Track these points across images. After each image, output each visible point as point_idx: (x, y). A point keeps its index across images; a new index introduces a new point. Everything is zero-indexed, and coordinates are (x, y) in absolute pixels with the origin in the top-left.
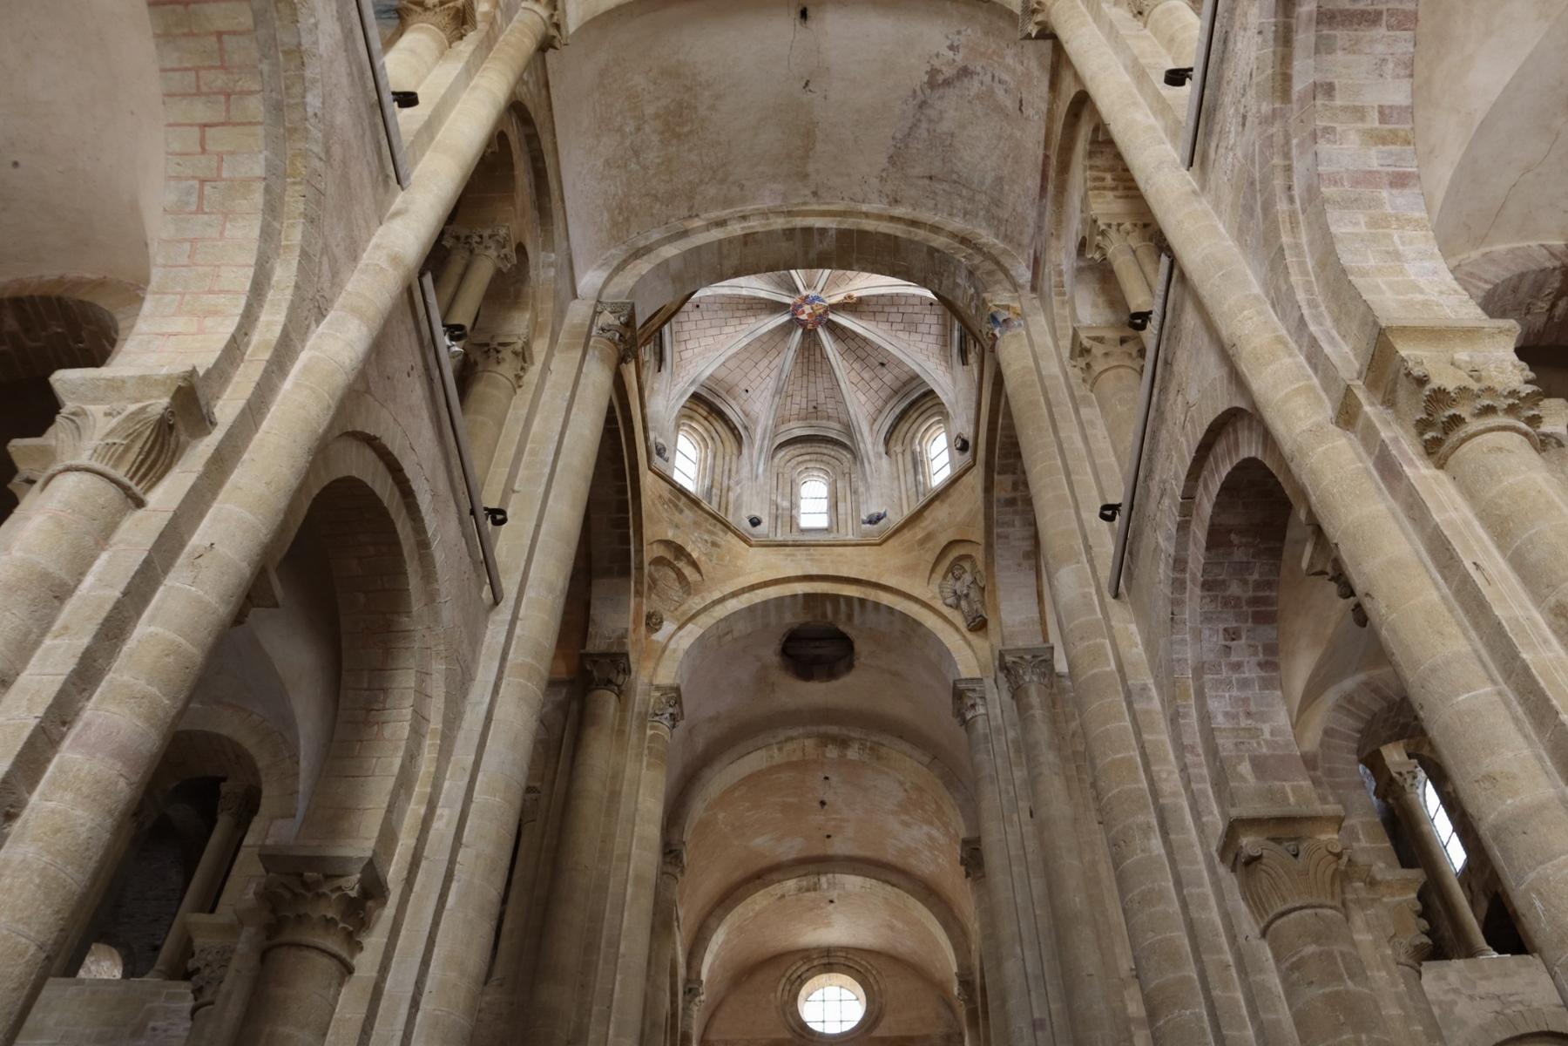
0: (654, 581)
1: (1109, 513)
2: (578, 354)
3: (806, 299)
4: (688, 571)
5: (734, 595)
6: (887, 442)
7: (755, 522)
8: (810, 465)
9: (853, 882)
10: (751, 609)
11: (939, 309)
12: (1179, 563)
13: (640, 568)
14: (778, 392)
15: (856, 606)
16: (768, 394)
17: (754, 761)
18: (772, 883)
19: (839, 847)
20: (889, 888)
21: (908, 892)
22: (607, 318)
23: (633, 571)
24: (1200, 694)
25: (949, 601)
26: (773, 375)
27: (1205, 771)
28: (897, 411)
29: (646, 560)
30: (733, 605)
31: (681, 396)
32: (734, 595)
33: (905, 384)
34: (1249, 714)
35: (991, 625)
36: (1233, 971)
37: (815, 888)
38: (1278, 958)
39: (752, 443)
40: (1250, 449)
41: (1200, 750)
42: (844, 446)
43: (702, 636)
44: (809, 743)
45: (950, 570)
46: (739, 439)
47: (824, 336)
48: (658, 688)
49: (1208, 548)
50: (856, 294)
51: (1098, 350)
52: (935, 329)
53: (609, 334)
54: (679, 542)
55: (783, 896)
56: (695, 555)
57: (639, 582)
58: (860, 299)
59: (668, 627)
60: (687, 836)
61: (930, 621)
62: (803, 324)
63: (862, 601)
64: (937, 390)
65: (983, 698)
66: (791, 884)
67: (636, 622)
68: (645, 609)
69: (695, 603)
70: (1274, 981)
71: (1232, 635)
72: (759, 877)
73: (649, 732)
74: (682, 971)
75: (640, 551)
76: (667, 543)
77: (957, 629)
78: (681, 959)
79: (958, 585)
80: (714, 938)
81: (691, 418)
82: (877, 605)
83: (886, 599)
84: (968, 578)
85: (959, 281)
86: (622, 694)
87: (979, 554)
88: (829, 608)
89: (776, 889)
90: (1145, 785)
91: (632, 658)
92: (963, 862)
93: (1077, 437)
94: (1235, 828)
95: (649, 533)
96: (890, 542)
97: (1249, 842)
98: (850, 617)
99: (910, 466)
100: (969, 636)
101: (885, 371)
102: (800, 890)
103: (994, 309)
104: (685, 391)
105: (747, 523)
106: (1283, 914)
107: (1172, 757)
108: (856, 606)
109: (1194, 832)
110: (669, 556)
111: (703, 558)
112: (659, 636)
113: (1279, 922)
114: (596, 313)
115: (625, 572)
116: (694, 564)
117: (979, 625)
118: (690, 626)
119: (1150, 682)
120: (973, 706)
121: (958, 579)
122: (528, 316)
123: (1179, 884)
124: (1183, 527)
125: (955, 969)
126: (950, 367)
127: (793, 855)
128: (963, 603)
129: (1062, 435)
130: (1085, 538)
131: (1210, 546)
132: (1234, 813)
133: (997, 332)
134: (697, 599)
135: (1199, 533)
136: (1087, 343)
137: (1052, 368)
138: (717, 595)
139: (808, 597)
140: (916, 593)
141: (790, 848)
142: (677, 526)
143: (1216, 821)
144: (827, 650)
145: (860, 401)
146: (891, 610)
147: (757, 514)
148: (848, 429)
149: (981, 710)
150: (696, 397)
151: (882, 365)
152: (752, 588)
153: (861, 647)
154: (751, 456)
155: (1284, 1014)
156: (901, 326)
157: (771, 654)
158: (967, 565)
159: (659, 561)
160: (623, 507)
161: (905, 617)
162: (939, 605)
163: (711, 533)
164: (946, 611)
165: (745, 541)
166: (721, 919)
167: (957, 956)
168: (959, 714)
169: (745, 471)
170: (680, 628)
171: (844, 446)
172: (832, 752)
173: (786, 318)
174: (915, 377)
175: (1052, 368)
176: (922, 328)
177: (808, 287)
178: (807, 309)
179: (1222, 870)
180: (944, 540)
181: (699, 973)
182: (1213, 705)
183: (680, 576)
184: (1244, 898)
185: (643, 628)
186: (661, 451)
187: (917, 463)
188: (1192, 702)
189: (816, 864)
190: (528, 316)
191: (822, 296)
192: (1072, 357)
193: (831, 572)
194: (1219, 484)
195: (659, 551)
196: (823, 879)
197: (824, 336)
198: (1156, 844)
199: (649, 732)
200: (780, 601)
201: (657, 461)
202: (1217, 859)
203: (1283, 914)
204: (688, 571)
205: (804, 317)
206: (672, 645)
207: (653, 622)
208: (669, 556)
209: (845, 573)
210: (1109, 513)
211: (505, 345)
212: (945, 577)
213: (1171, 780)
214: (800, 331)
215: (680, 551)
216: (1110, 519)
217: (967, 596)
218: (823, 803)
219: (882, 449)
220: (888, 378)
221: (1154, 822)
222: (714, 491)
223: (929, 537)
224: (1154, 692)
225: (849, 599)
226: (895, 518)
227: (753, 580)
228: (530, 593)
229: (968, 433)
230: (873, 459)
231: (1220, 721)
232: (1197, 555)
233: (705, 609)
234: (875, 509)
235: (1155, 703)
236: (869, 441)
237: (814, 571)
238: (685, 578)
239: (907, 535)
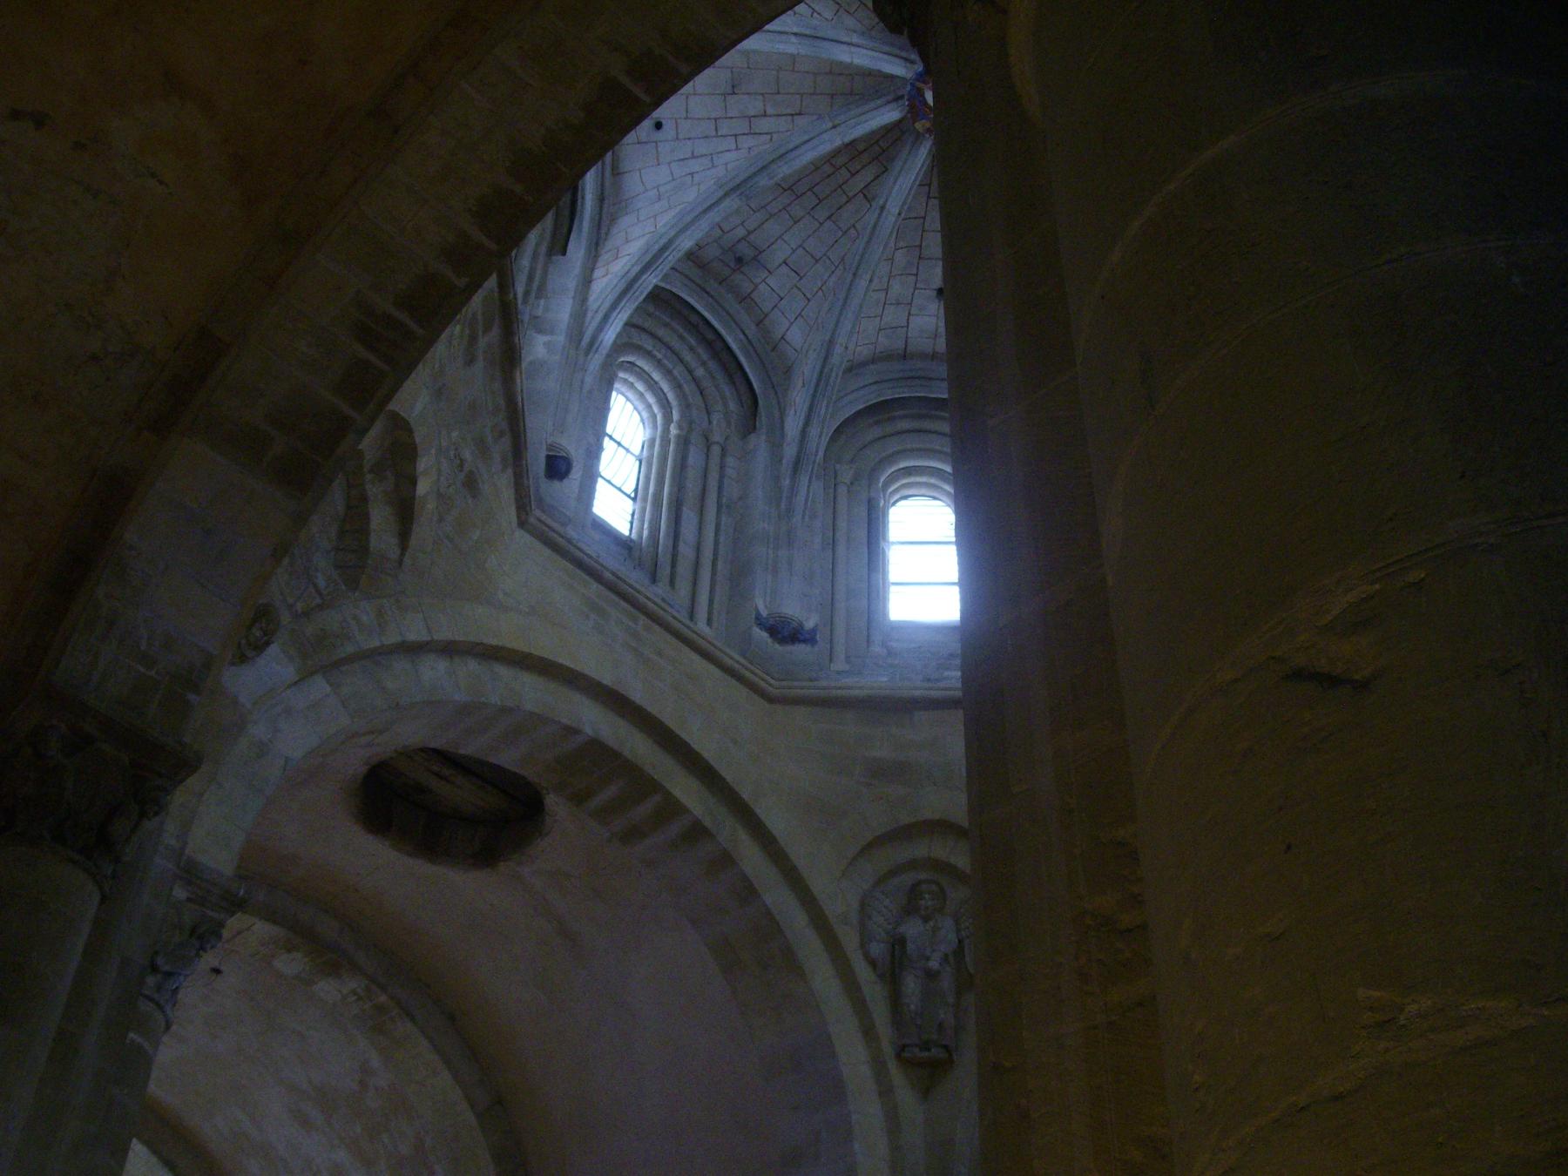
4: (380, 517)
14: (739, 188)
61: (823, 978)
63: (697, 832)
77: (869, 1032)
82: (725, 860)
100: (893, 1067)
116: (405, 511)
138: (415, 631)
154: (587, 281)
157: (355, 762)
162: (850, 940)
163: (483, 449)
164: (864, 973)
183: (355, 523)
193: (666, 711)
204: (380, 517)
217: (931, 975)
225: (671, 809)
227: (507, 631)
237: (637, 693)
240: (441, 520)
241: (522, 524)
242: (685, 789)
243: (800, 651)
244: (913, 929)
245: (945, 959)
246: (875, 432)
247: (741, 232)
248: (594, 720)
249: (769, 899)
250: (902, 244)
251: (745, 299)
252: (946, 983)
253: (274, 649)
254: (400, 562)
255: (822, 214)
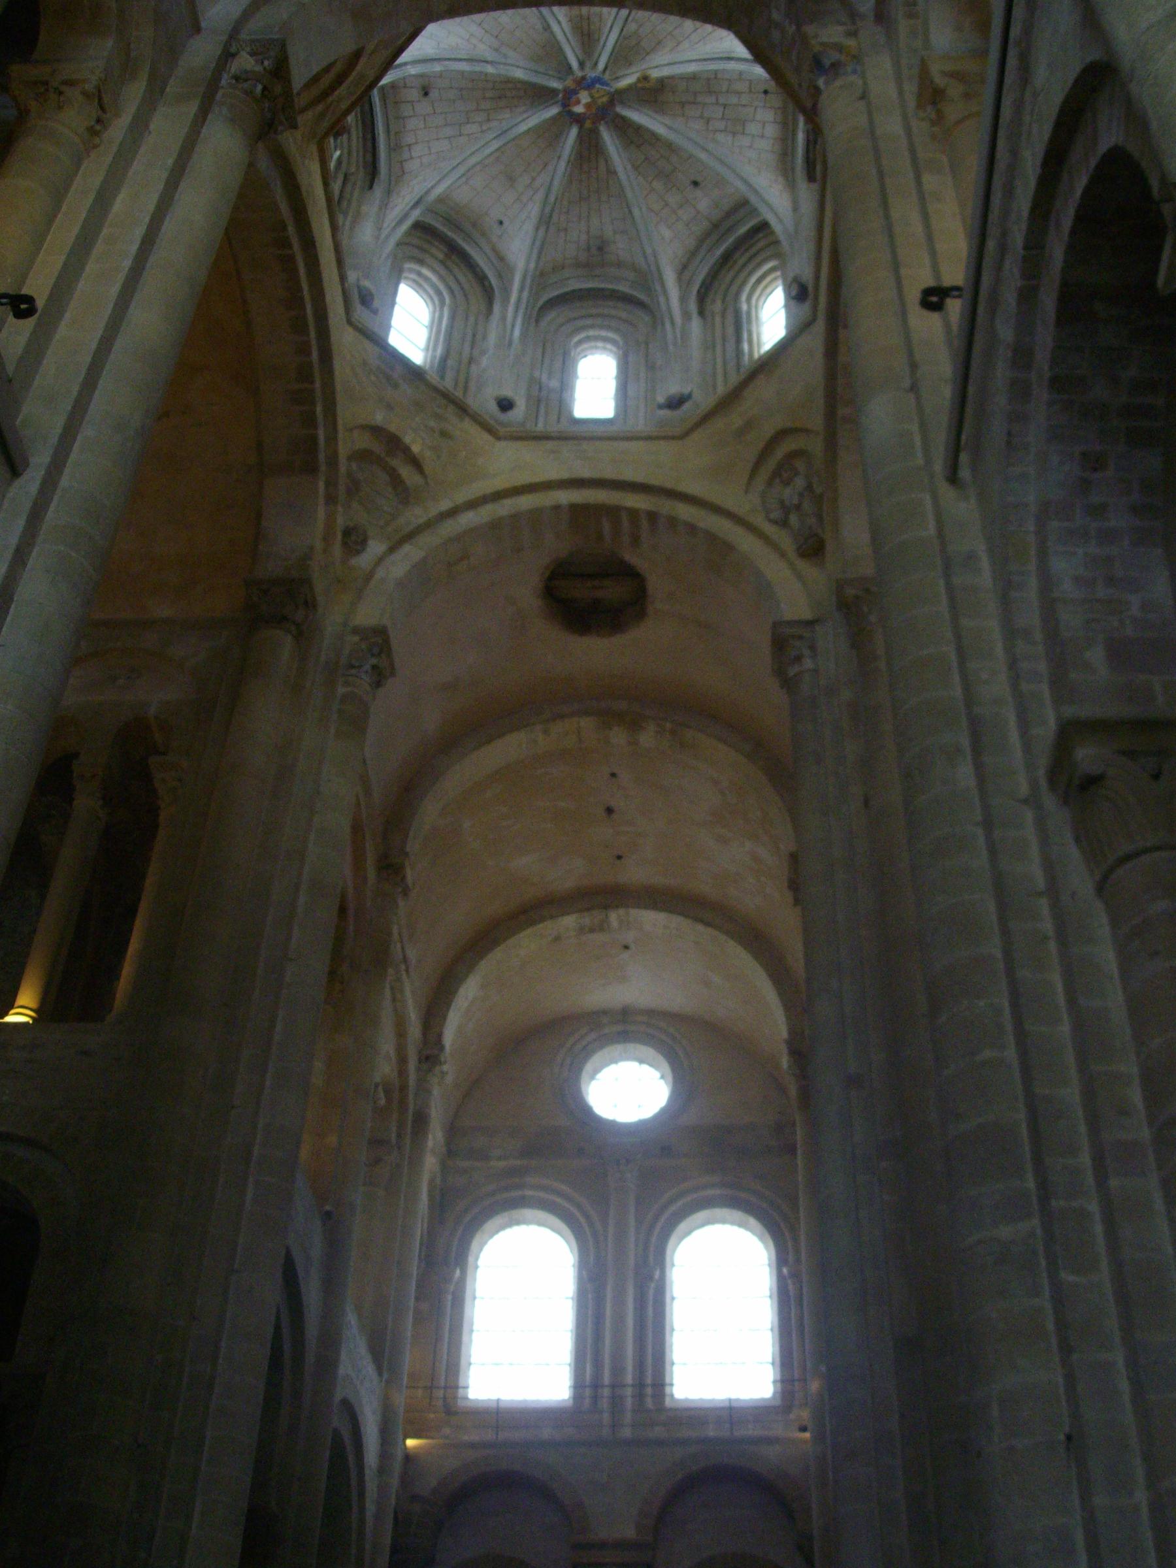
0: (354, 487)
1: (934, 299)
2: (192, 108)
3: (584, 83)
5: (472, 505)
6: (702, 299)
7: (505, 405)
8: (591, 333)
9: (651, 920)
10: (495, 525)
11: (776, 100)
12: (1022, 356)
13: (333, 461)
14: (545, 221)
15: (645, 524)
16: (529, 227)
17: (511, 747)
18: (542, 919)
19: (635, 873)
20: (700, 927)
21: (727, 933)
22: (245, 62)
23: (323, 468)
24: (1043, 555)
25: (772, 516)
26: (540, 196)
27: (1042, 667)
28: (719, 252)
29: (343, 451)
30: (468, 519)
31: (400, 222)
32: (472, 505)
33: (728, 214)
34: (1110, 581)
35: (830, 546)
36: (1052, 946)
37: (602, 927)
38: (1115, 922)
39: (506, 300)
40: (1109, 134)
41: (1038, 636)
42: (641, 304)
43: (424, 560)
44: (587, 723)
45: (776, 473)
46: (488, 294)
47: (607, 137)
48: (356, 631)
49: (1059, 323)
50: (655, 74)
51: (955, 90)
52: (772, 131)
53: (246, 85)
54: (392, 428)
55: (557, 939)
56: (416, 449)
57: (331, 483)
58: (662, 82)
59: (375, 547)
60: (413, 846)
61: (746, 543)
62: (578, 120)
63: (653, 516)
64: (773, 222)
65: (812, 648)
66: (569, 921)
67: (327, 539)
68: (340, 521)
69: (416, 515)
70: (1107, 956)
71: (1093, 462)
72: (524, 912)
73: (341, 690)
74: (415, 1031)
75: (332, 438)
76: (376, 431)
77: (783, 555)
78: (413, 1016)
79: (787, 492)
80: (462, 991)
81: (421, 262)
82: (673, 522)
83: (684, 512)
84: (800, 482)
85: (776, 16)
86: (304, 635)
87: (816, 446)
88: (607, 527)
89: (548, 928)
90: (958, 692)
91: (319, 585)
92: (789, 887)
93: (915, 217)
94: (1069, 733)
95: (346, 413)
96: (696, 436)
97: (1088, 756)
98: (636, 540)
99: (730, 330)
101: (698, 193)
102: (581, 930)
103: (817, 48)
104: (406, 216)
105: (493, 407)
106: (1128, 858)
107: (999, 649)
108: (645, 524)
109: (1018, 754)
110: (377, 448)
111: (428, 454)
112: (364, 560)
113: (1120, 872)
114: (227, 55)
115: (311, 468)
116: (416, 463)
117: (813, 548)
118: (407, 548)
119: (981, 548)
120: (798, 659)
121: (787, 483)
122: (110, 43)
123: (988, 824)
124: (1028, 296)
125: (785, 1034)
126: (791, 185)
127: (570, 884)
128: (794, 519)
129: (895, 214)
130: (911, 354)
131: (1061, 321)
132: (1070, 711)
133: (821, 82)
134: (418, 511)
135: (1048, 301)
136: (939, 81)
137: (891, 126)
138: (445, 505)
139: (577, 510)
140: (730, 504)
141: (567, 874)
142: (389, 407)
143: (1047, 728)
144: (612, 592)
145: (665, 242)
146: (692, 528)
147: (507, 392)
148: (647, 278)
149: (808, 663)
150: (418, 226)
151: (695, 184)
152: (498, 496)
153: (657, 584)
154: (503, 318)
155: (1114, 1000)
156: (721, 125)
158: (800, 465)
159: (363, 456)
160: (304, 374)
161: (712, 537)
162: (759, 521)
163: (438, 417)
165: (489, 430)
166: (471, 968)
167: (788, 1018)
168: (780, 672)
169: (492, 337)
170: (392, 549)
171: (641, 304)
172: (618, 737)
173: (554, 111)
174: (742, 206)
175: (891, 126)
176: (753, 128)
177: (582, 65)
178: (584, 97)
179: (1050, 801)
180: (768, 429)
181: (440, 1036)
182: (1060, 565)
183: (396, 481)
184: (1077, 840)
185: (337, 550)
186: (366, 299)
187: (740, 325)
188: (1032, 566)
189: (602, 897)
190: (110, 43)
191: (607, 77)
192: (919, 106)
193: (609, 473)
194: (1071, 212)
195: (363, 441)
196: (614, 917)
197: (607, 137)
198: (965, 774)
199: (341, 690)
200: (535, 517)
201: (361, 314)
202: (1043, 783)
203: (1128, 858)
205: (579, 109)
206: (380, 573)
207: (354, 540)
208: (377, 448)
209: (629, 474)
210: (934, 299)
211: (70, 83)
212: (769, 484)
213: (995, 684)
214: (574, 131)
215: (394, 444)
216: (937, 307)
217: (798, 507)
218: (610, 811)
219: (693, 307)
220: (703, 204)
221: (965, 742)
222: (450, 362)
223: (748, 426)
224: (985, 563)
225: (633, 513)
226: (703, 400)
227: (499, 483)
228: (87, 432)
229: (807, 275)
230: (678, 320)
231: (1067, 588)
232: (1045, 338)
233: (429, 525)
234: (674, 388)
235: (985, 577)
236: (672, 294)
237: (586, 473)
238: (402, 482)
239: (719, 423)
240: (439, 457)
241: (499, 438)
242: (632, 501)
243: (687, 406)
244: (789, 494)
245: (801, 495)
246: (732, 273)
247: (584, 237)
248: (565, 497)
249: (701, 525)
250: (650, 179)
251: (619, 264)
252: (807, 506)
253: (371, 543)
254: (427, 483)
255: (604, 198)
